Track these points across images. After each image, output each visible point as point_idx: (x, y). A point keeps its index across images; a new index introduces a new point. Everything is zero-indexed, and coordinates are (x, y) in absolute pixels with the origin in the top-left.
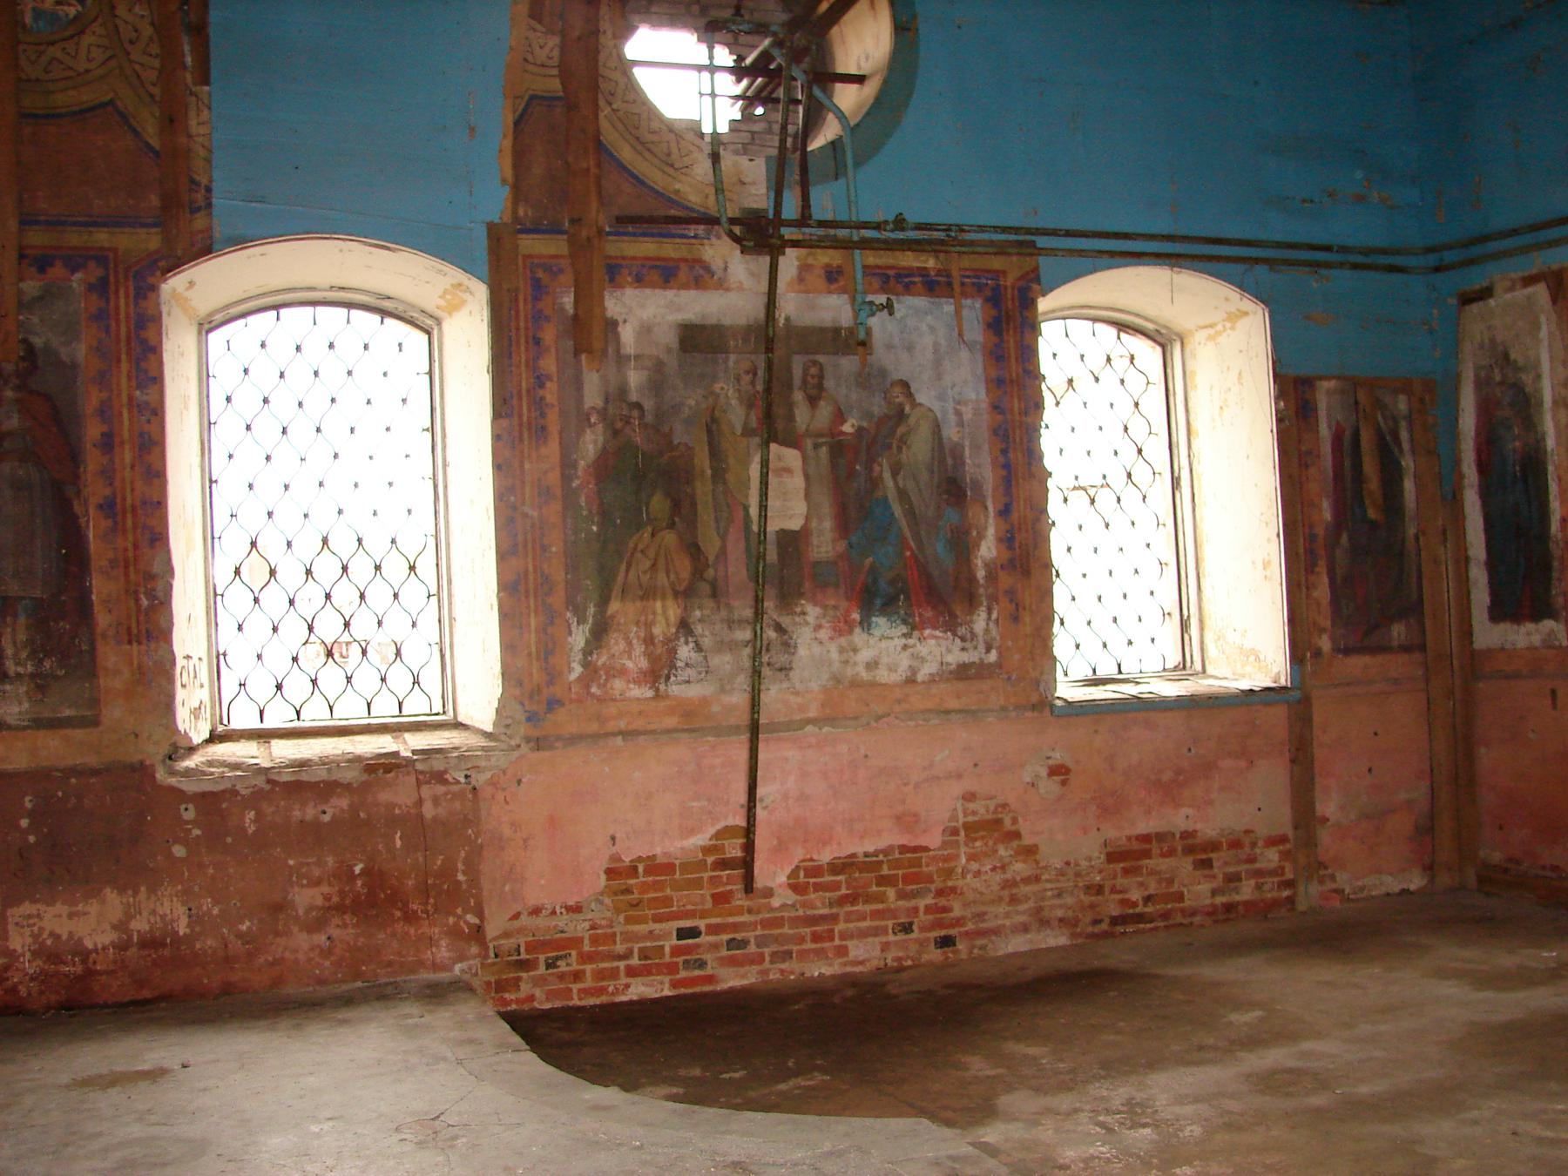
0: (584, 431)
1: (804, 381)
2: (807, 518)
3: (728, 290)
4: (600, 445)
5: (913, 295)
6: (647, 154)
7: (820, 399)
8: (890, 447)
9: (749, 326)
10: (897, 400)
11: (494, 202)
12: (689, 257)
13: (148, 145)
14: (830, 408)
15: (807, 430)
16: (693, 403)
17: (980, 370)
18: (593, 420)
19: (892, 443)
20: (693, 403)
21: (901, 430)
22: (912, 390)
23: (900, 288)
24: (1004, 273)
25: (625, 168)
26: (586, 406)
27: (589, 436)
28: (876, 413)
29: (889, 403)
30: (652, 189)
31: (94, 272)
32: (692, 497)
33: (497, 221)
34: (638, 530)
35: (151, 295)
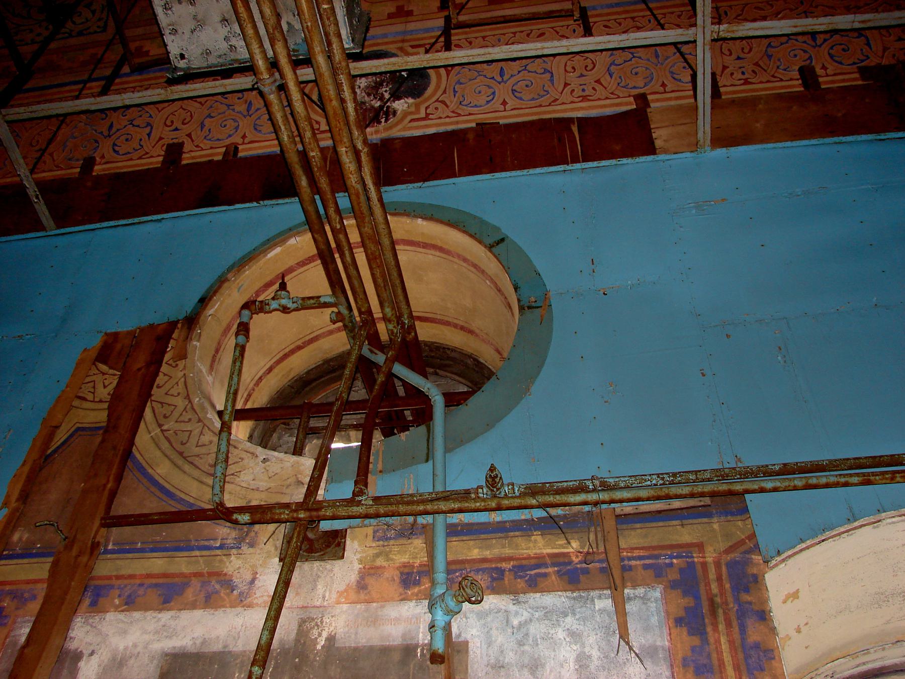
6: (187, 467)
23: (521, 583)
24: (700, 547)
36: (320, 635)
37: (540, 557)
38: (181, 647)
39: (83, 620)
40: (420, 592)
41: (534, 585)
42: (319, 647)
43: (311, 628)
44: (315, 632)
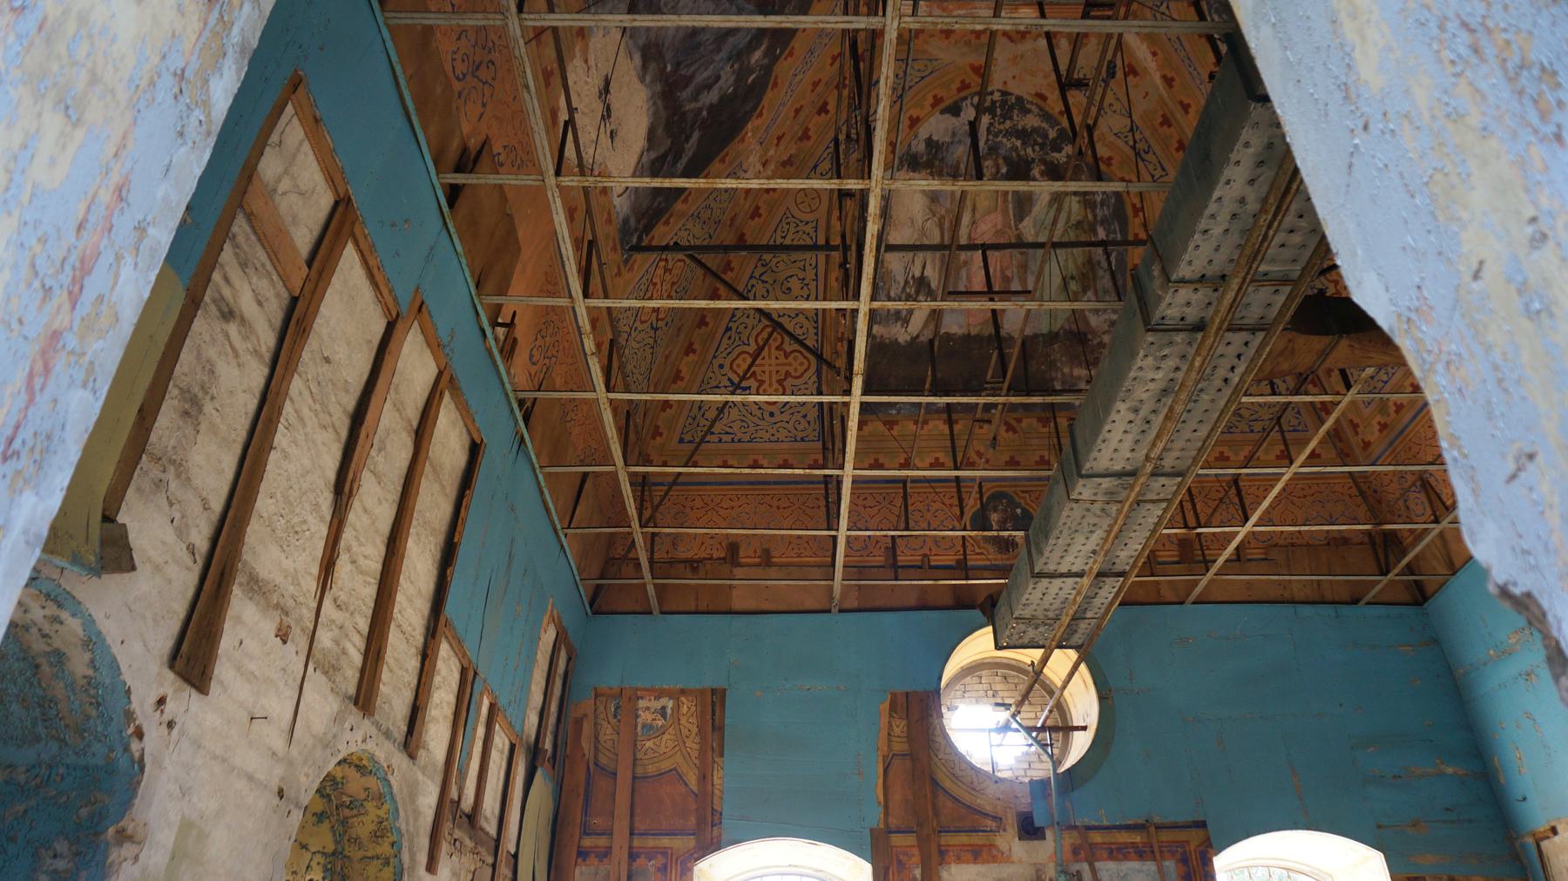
3: (1013, 862)
5: (1130, 860)
6: (960, 784)
11: (875, 817)
12: (987, 843)
13: (692, 791)
23: (1120, 856)
24: (1188, 842)
25: (945, 791)
30: (963, 804)
31: (661, 860)
33: (876, 826)
35: (688, 874)
37: (1126, 843)
41: (1126, 858)
44: (1043, 877)
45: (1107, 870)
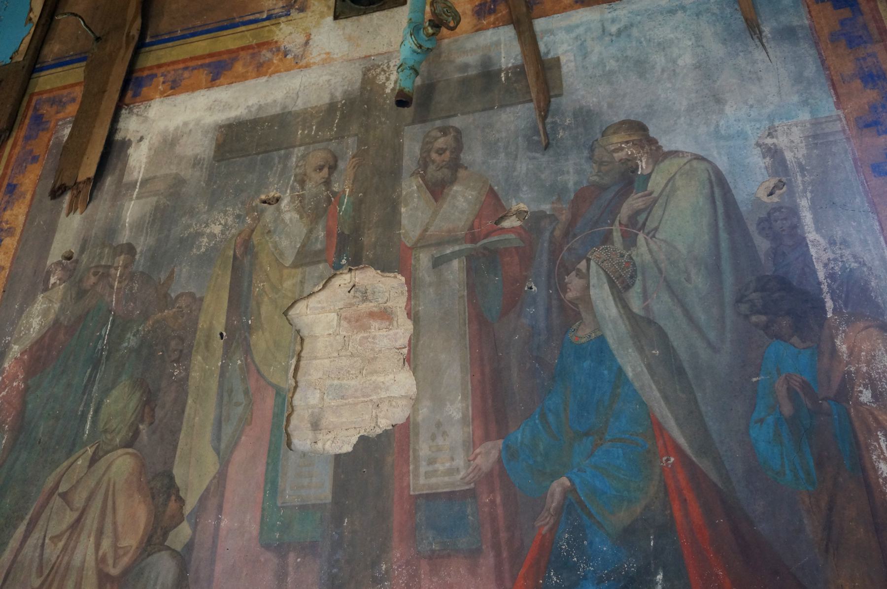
0: (34, 299)
1: (424, 163)
2: (416, 402)
4: (52, 316)
7: (453, 180)
8: (607, 238)
9: (332, 107)
10: (617, 156)
14: (471, 194)
15: (422, 237)
16: (217, 229)
17: (811, 68)
18: (53, 280)
19: (610, 232)
20: (217, 229)
21: (634, 202)
22: (653, 132)
26: (49, 263)
27: (40, 304)
28: (571, 185)
29: (601, 163)
32: (183, 383)
34: (69, 455)
36: (388, 79)
38: (236, 117)
39: (127, 111)
40: (497, 19)
42: (388, 91)
43: (377, 75)
44: (382, 77)
45: (569, 29)
